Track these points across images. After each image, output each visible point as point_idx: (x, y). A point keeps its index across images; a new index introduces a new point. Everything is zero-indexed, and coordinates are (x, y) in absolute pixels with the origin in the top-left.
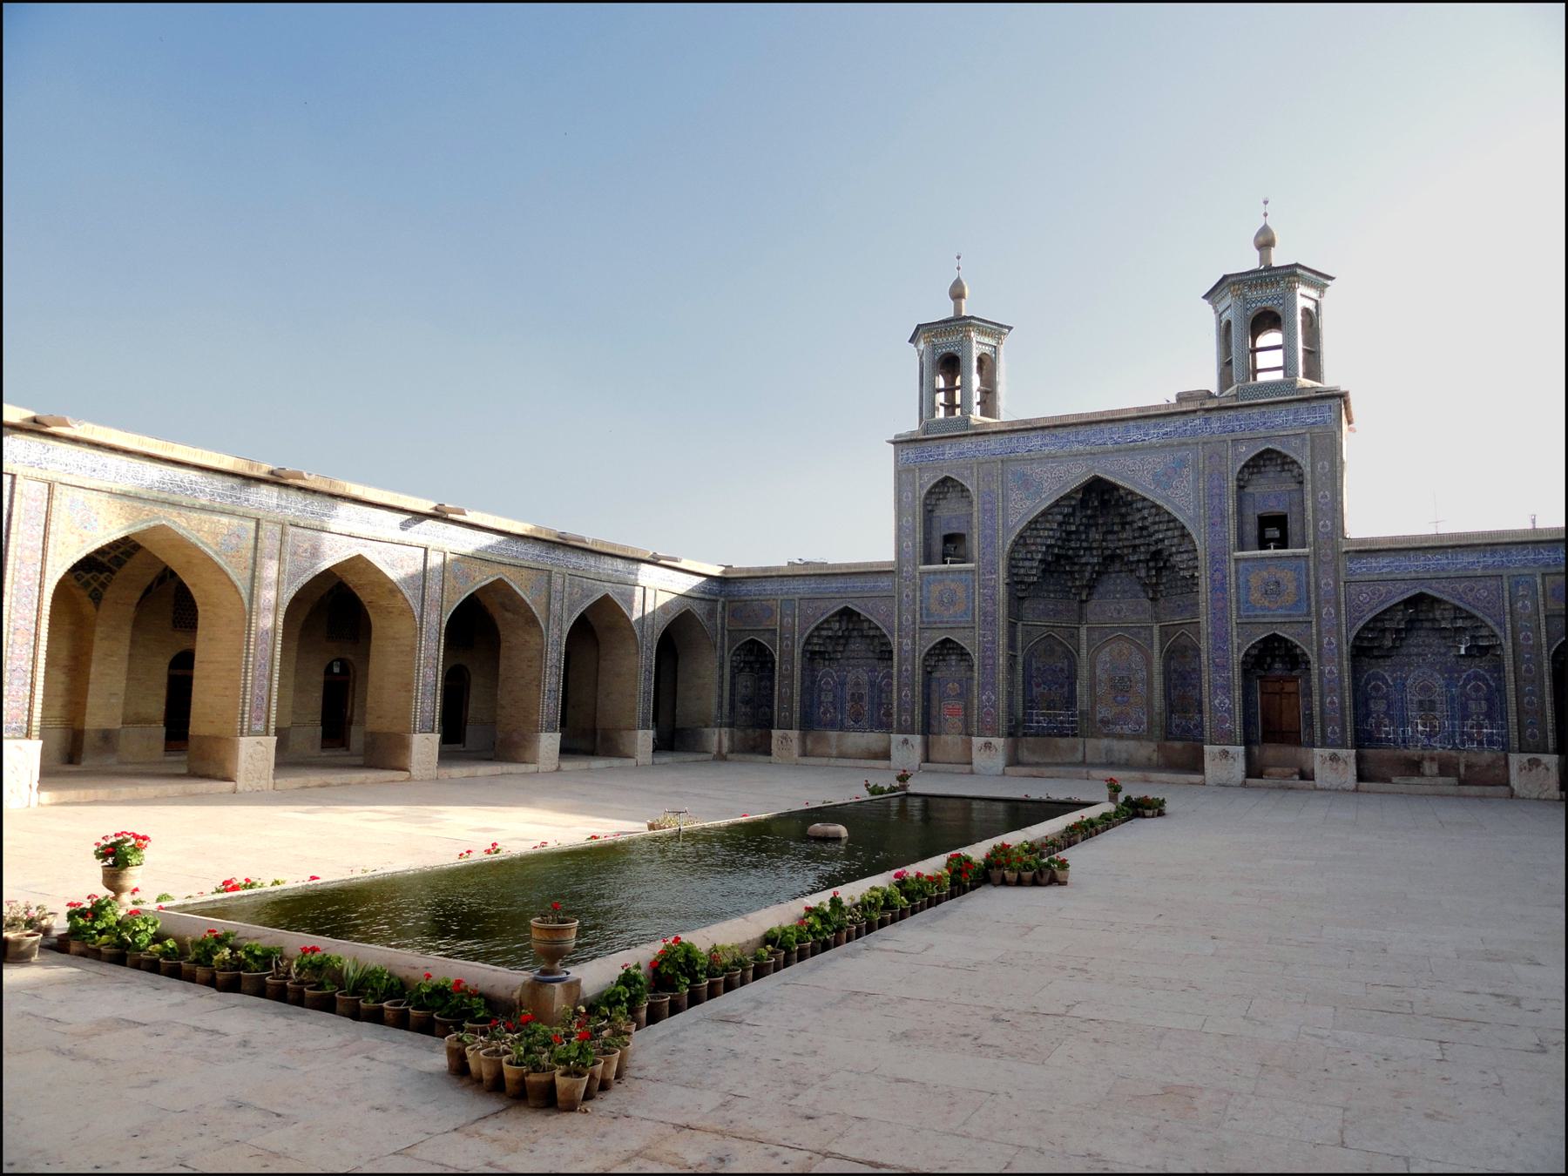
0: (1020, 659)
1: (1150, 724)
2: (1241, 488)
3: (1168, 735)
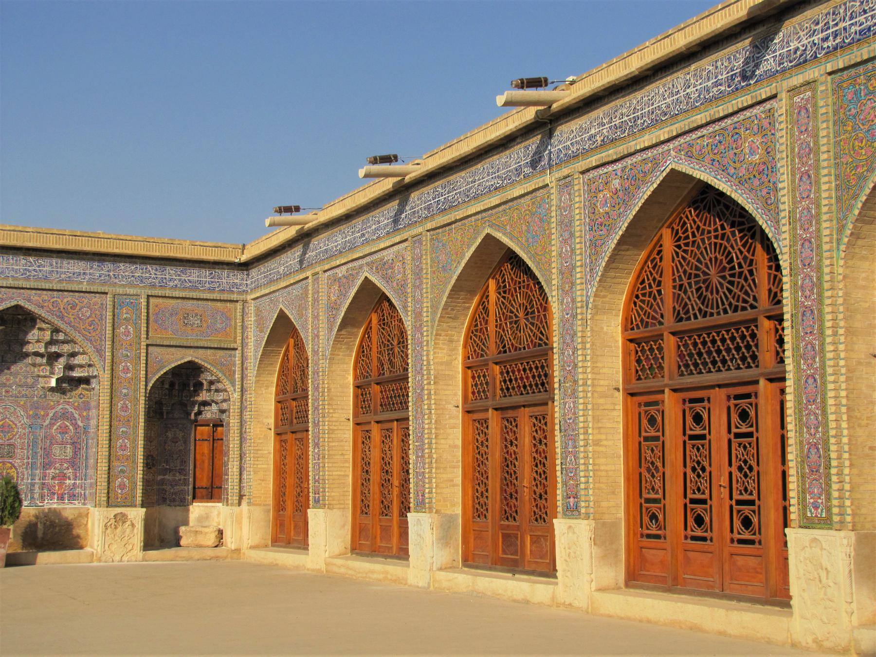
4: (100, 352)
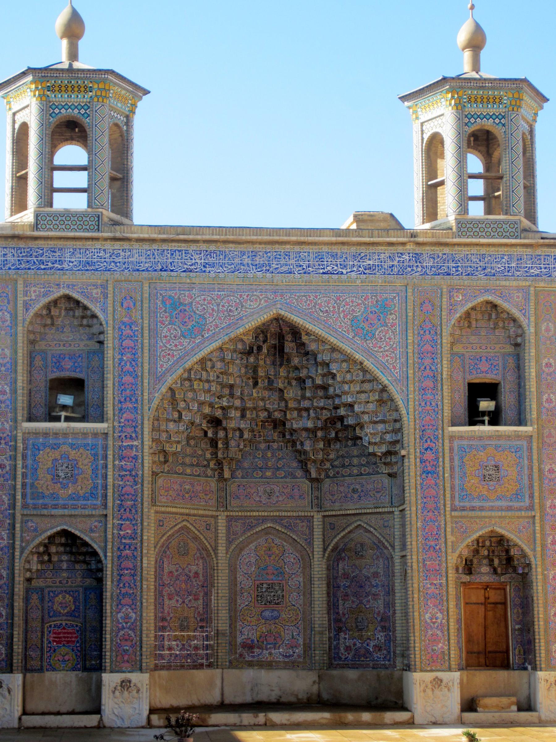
1: (307, 647)
2: (452, 344)
3: (334, 660)
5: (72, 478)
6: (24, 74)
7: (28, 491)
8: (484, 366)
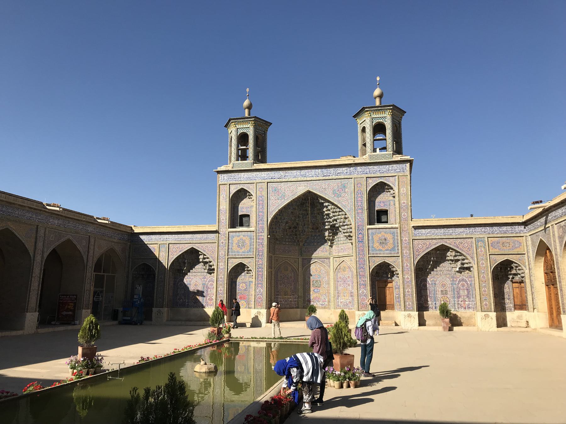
0: (273, 273)
1: (329, 302)
4: (472, 258)
5: (243, 246)
6: (230, 120)
7: (230, 250)
8: (382, 205)
